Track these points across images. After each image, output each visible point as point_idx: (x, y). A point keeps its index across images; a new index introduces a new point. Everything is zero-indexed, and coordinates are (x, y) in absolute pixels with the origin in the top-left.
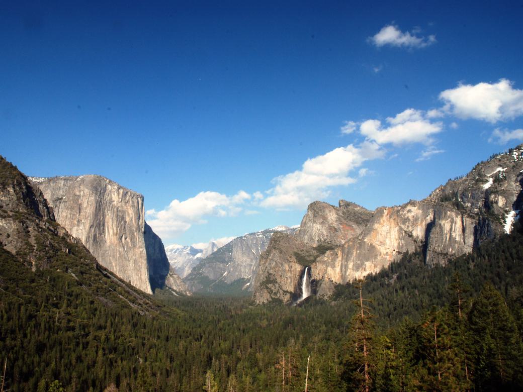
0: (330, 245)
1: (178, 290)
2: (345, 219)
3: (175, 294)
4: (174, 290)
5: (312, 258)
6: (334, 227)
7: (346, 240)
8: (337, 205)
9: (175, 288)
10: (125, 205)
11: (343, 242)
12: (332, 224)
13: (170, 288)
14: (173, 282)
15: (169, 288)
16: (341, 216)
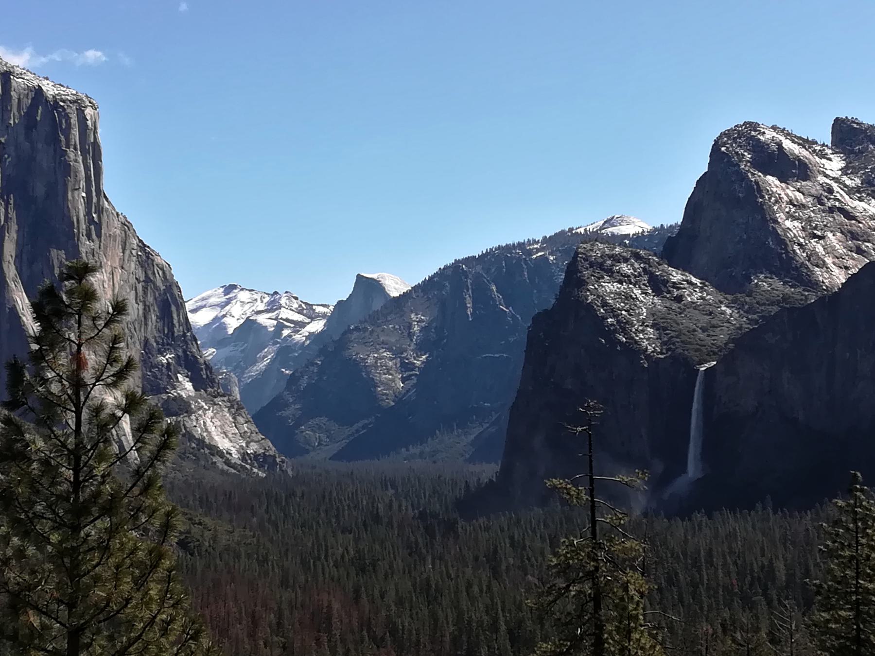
0: (789, 290)
1: (235, 455)
2: (850, 191)
3: (226, 467)
4: (220, 453)
5: (722, 337)
6: (809, 220)
7: (855, 271)
8: (826, 137)
9: (223, 444)
10: (28, 136)
11: (840, 277)
12: (802, 206)
13: (201, 442)
14: (219, 423)
15: (198, 440)
16: (834, 179)
